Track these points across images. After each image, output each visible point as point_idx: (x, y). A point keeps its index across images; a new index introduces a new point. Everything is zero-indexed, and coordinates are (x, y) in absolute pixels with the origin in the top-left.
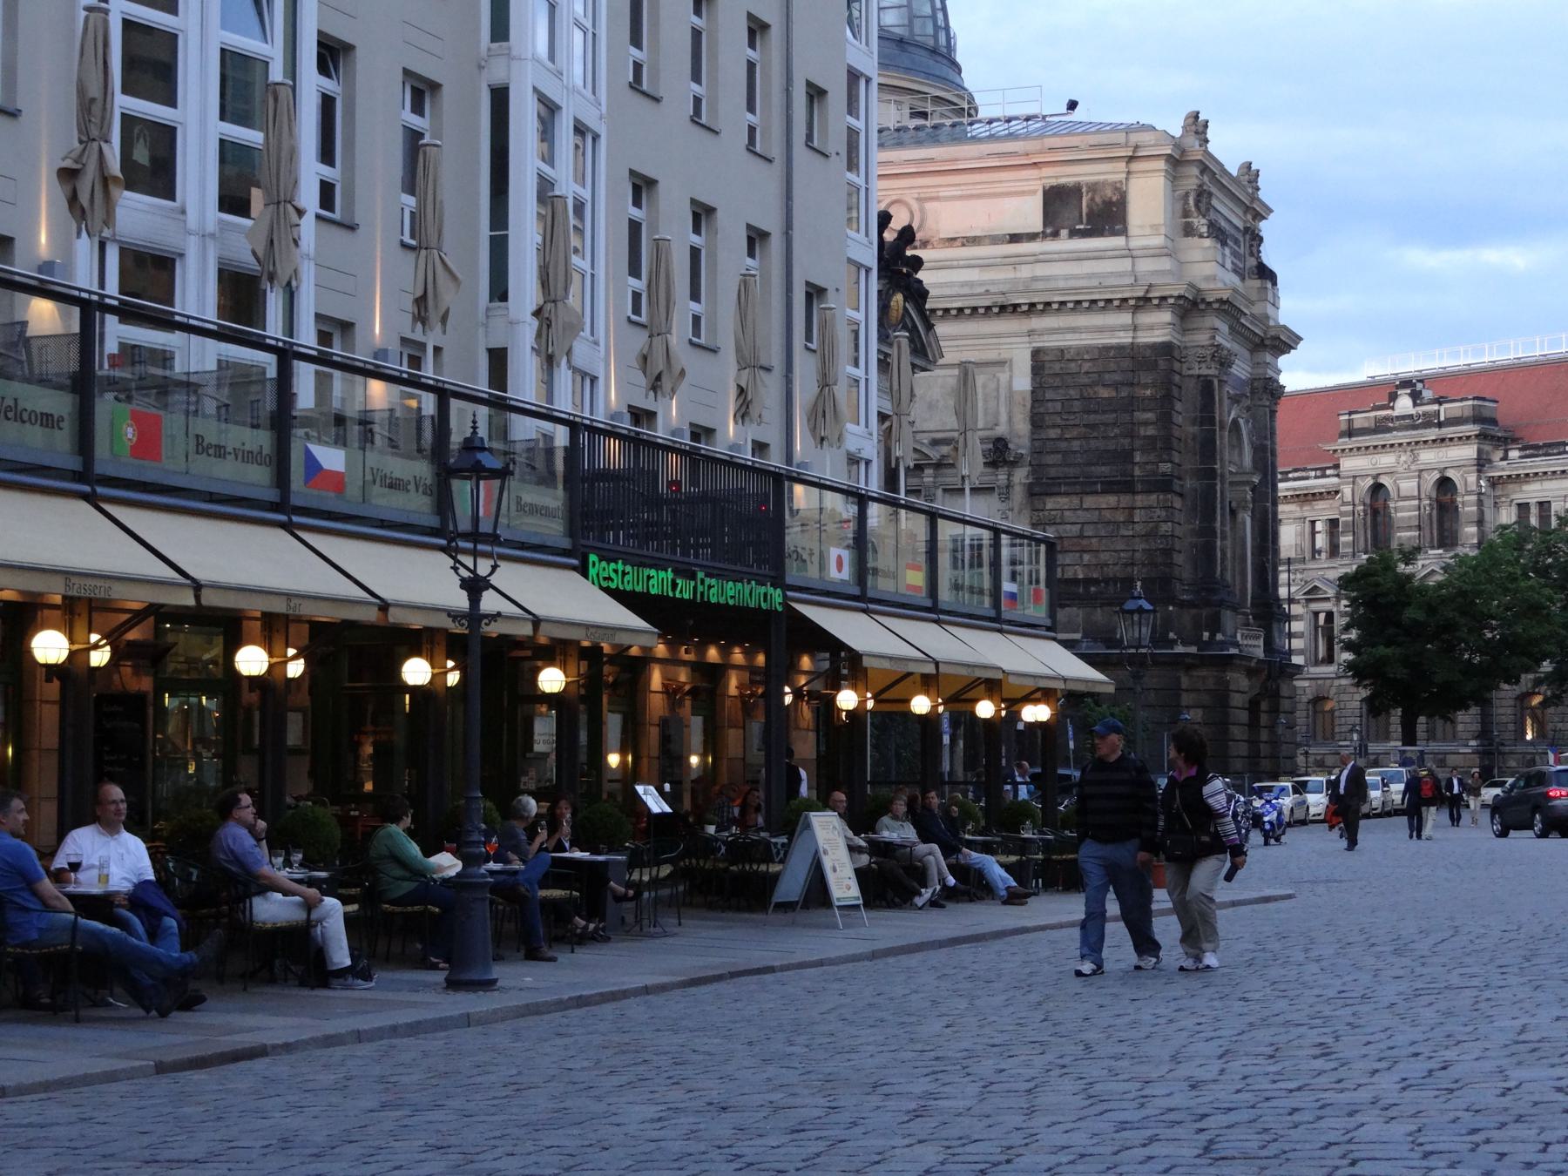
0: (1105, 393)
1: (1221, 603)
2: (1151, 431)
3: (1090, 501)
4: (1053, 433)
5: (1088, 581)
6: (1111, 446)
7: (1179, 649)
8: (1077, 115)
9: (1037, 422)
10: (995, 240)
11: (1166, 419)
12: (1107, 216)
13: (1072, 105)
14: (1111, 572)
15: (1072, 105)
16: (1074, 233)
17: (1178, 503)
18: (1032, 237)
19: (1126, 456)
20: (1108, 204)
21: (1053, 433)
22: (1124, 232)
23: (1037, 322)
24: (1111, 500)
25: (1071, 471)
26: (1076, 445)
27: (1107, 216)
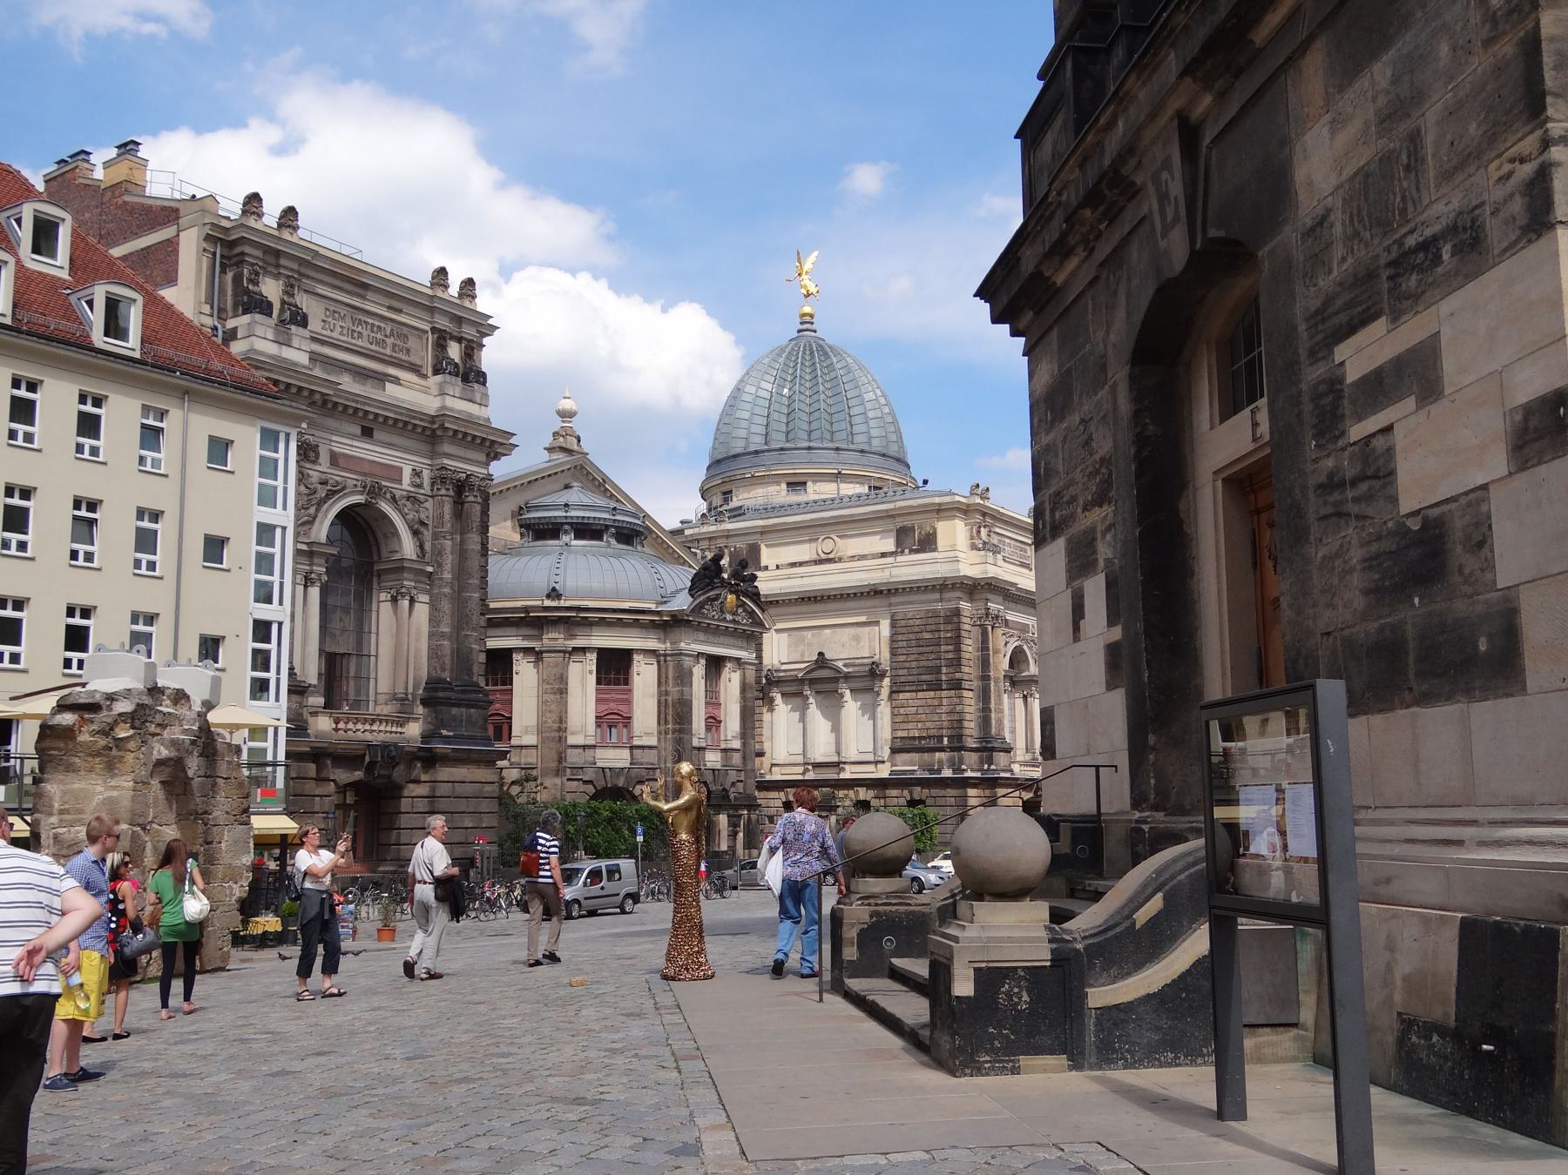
0: (927, 636)
1: (993, 749)
2: (951, 656)
3: (921, 695)
4: (902, 658)
5: (921, 738)
6: (930, 664)
7: (969, 774)
8: (929, 487)
9: (893, 653)
10: (874, 556)
11: (958, 650)
12: (928, 543)
13: (925, 482)
14: (932, 732)
15: (925, 482)
16: (912, 551)
17: (965, 693)
18: (892, 554)
19: (937, 670)
20: (928, 534)
21: (902, 658)
22: (935, 550)
23: (893, 600)
24: (932, 694)
25: (911, 678)
26: (914, 664)
27: (928, 543)
